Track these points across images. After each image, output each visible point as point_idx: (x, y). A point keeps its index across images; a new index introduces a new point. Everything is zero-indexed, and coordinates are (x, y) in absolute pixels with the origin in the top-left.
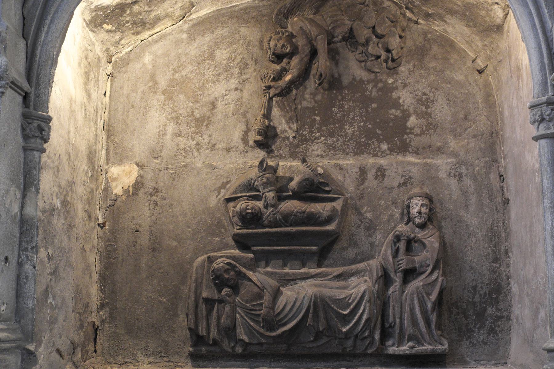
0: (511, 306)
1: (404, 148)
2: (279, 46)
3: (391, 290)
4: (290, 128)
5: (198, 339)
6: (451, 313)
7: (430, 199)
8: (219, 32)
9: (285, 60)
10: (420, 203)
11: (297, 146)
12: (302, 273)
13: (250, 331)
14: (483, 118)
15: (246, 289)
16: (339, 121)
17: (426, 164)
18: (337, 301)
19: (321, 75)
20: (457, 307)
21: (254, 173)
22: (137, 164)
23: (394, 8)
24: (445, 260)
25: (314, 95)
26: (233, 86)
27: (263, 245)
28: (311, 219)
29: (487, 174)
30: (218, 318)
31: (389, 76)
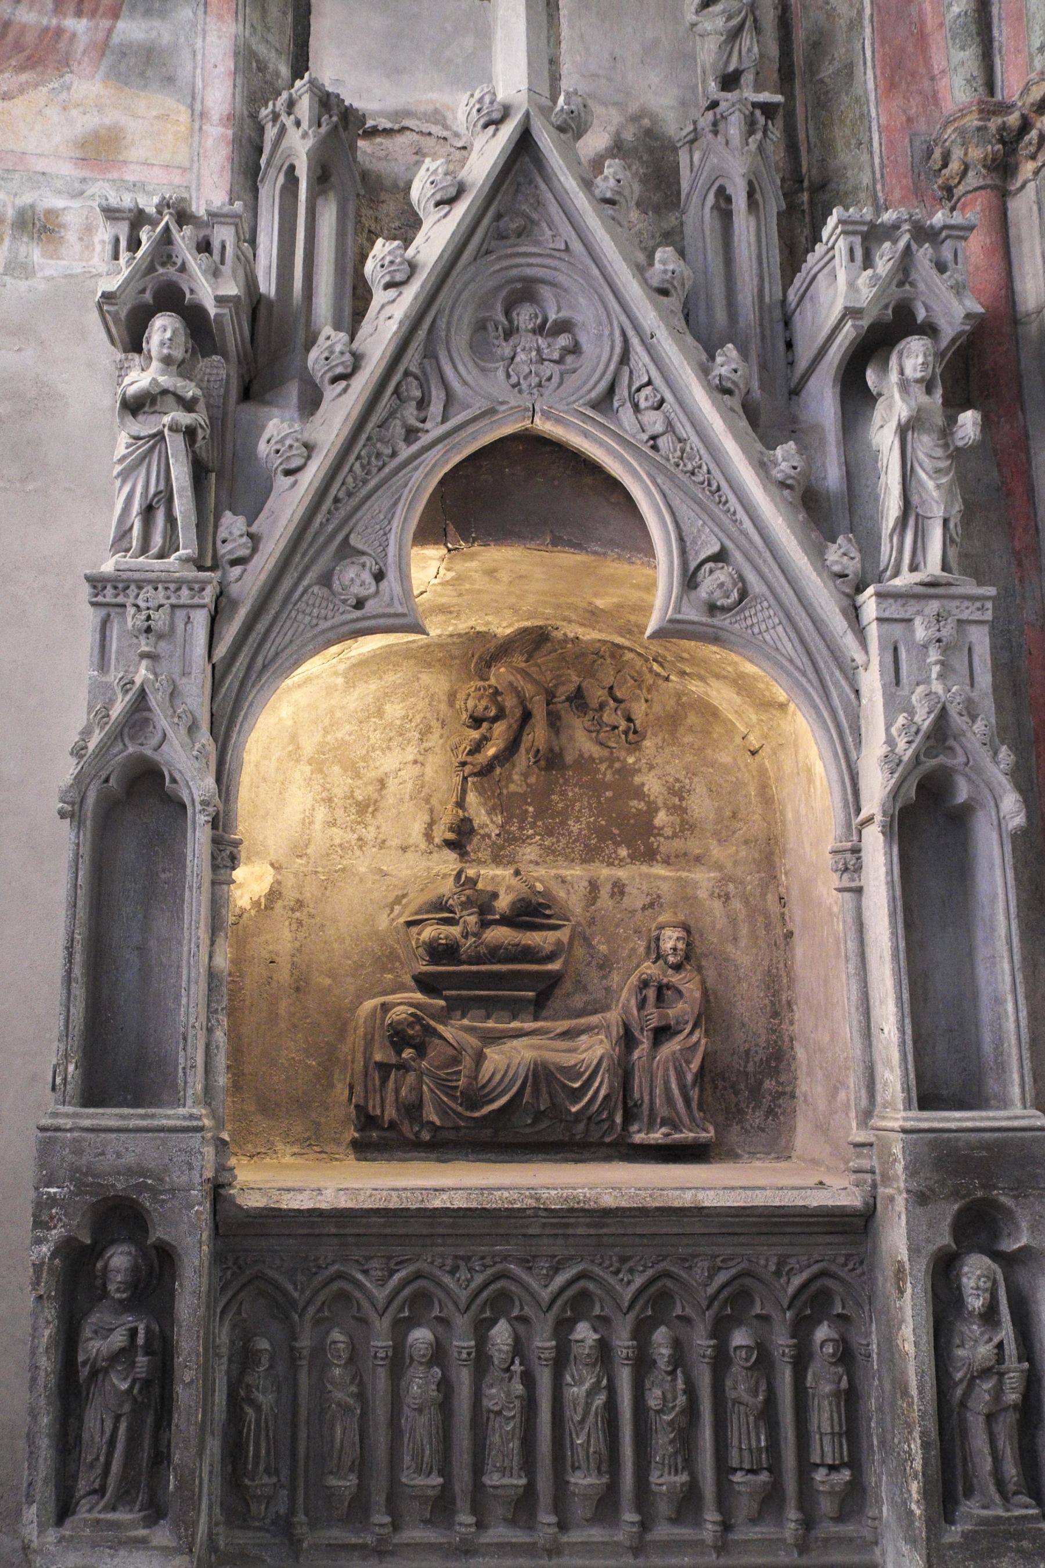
0: (796, 1079)
1: (650, 855)
2: (481, 708)
3: (636, 1055)
4: (493, 822)
5: (366, 1120)
6: (716, 1087)
7: (687, 930)
8: (390, 678)
9: (485, 725)
10: (676, 935)
11: (503, 848)
12: (512, 1029)
13: (443, 1110)
14: (756, 817)
15: (436, 1050)
16: (559, 814)
17: (680, 879)
18: (563, 1069)
19: (538, 751)
20: (724, 1079)
21: (447, 887)
22: (272, 865)
23: (639, 663)
24: (710, 1014)
25: (525, 775)
26: (411, 758)
27: (459, 989)
28: (527, 954)
29: (763, 895)
30: (397, 1091)
31: (630, 752)
